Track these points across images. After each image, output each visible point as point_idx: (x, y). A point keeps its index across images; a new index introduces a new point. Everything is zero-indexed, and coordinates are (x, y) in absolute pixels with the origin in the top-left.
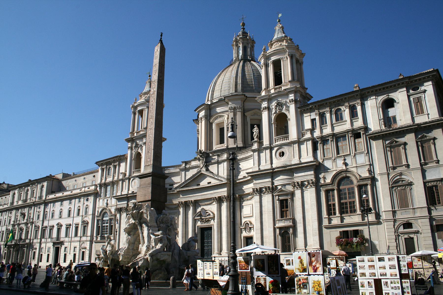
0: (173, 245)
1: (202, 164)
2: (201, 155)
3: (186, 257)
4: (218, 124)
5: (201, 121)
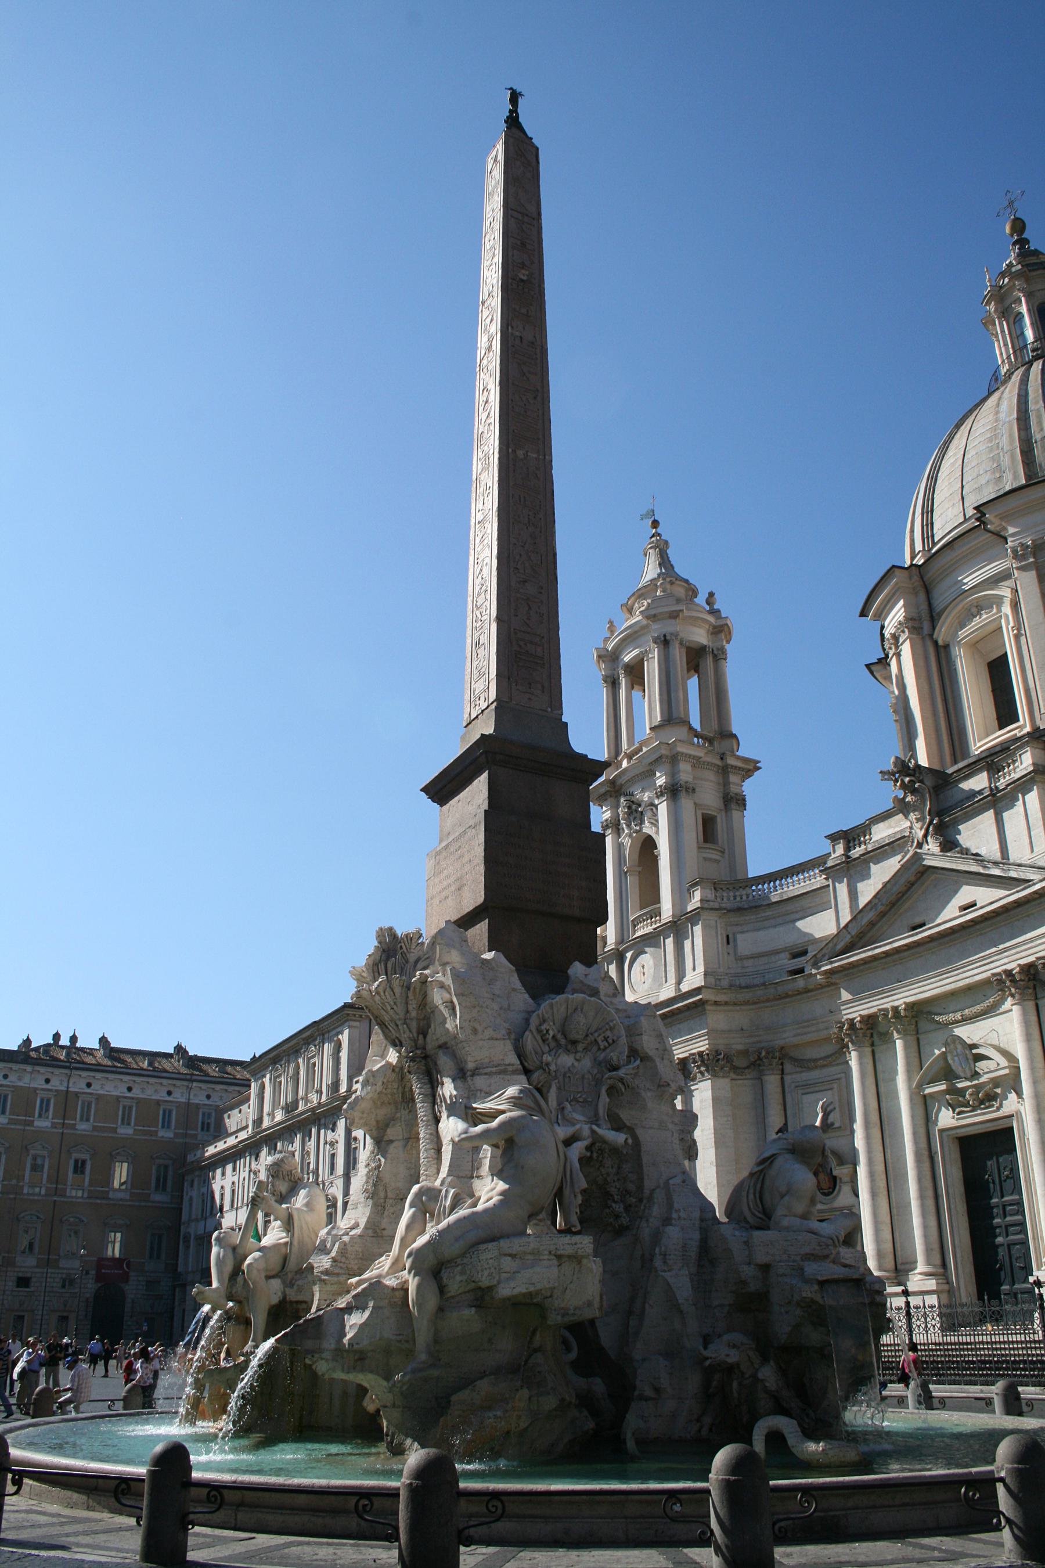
0: (659, 1196)
1: (919, 825)
2: (907, 779)
3: (748, 1272)
4: (975, 646)
5: (897, 647)
